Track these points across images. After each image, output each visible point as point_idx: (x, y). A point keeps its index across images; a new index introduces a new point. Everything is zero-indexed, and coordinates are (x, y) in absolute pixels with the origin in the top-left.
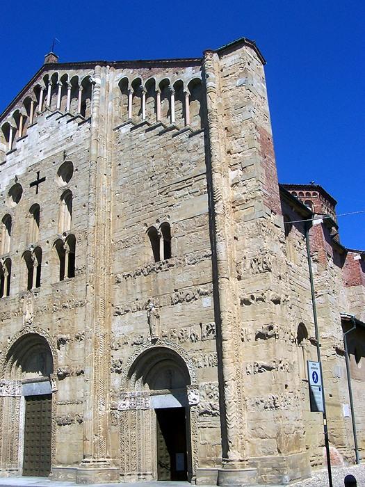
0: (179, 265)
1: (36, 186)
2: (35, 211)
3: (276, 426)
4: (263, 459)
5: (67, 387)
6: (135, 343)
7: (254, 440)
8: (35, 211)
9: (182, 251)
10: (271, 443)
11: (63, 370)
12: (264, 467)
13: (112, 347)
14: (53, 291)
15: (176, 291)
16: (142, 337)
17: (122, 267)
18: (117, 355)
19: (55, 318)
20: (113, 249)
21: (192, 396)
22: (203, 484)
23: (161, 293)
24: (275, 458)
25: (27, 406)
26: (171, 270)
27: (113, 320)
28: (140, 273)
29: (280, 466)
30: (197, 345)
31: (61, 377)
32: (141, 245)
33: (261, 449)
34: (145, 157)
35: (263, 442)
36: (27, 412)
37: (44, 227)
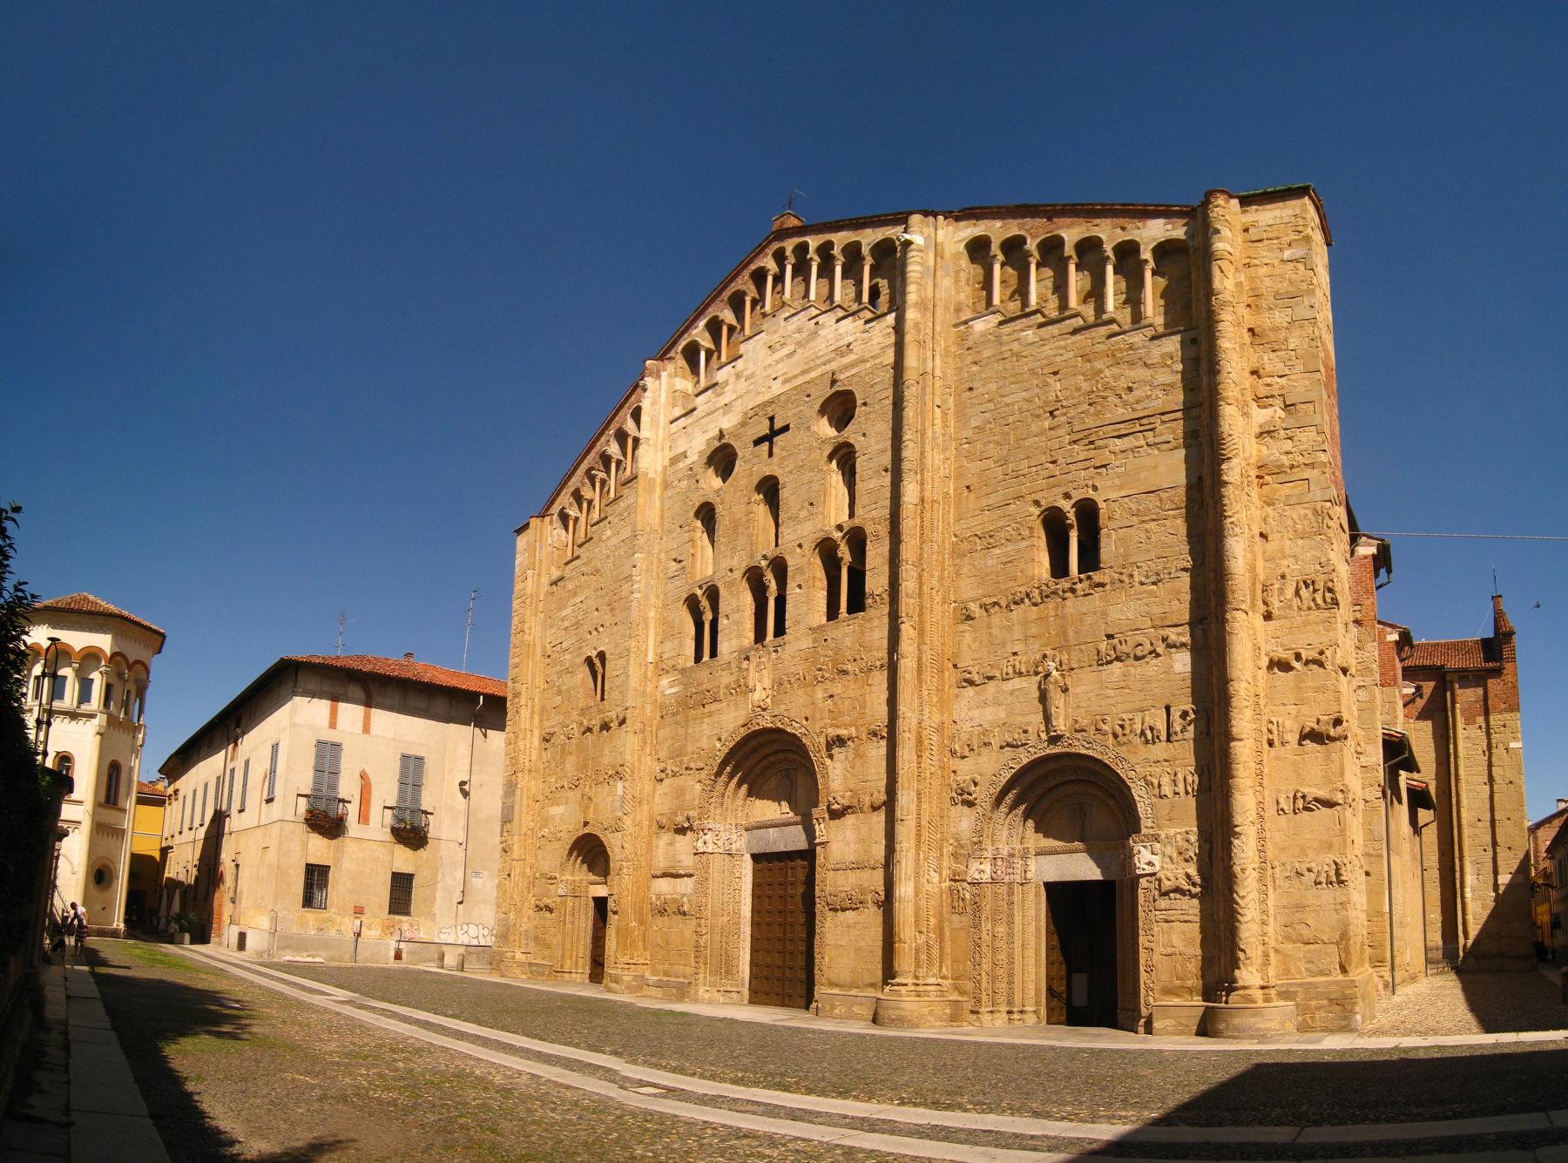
0: (1118, 585)
1: (767, 443)
2: (770, 489)
3: (1339, 921)
4: (1309, 983)
5: (850, 835)
6: (1009, 745)
7: (1289, 946)
8: (770, 489)
9: (1126, 556)
10: (1326, 954)
11: (839, 799)
12: (1312, 999)
13: (953, 753)
14: (815, 641)
15: (1110, 637)
16: (1025, 732)
17: (978, 587)
18: (966, 770)
19: (820, 694)
20: (957, 554)
21: (1145, 858)
22: (1169, 1033)
23: (1072, 641)
24: (1336, 983)
25: (756, 872)
26: (1098, 594)
27: (957, 696)
28: (1022, 601)
29: (1345, 997)
30: (1160, 750)
31: (836, 815)
32: (1025, 543)
33: (1303, 966)
34: (1037, 374)
35: (1309, 951)
36: (757, 885)
37: (790, 518)
